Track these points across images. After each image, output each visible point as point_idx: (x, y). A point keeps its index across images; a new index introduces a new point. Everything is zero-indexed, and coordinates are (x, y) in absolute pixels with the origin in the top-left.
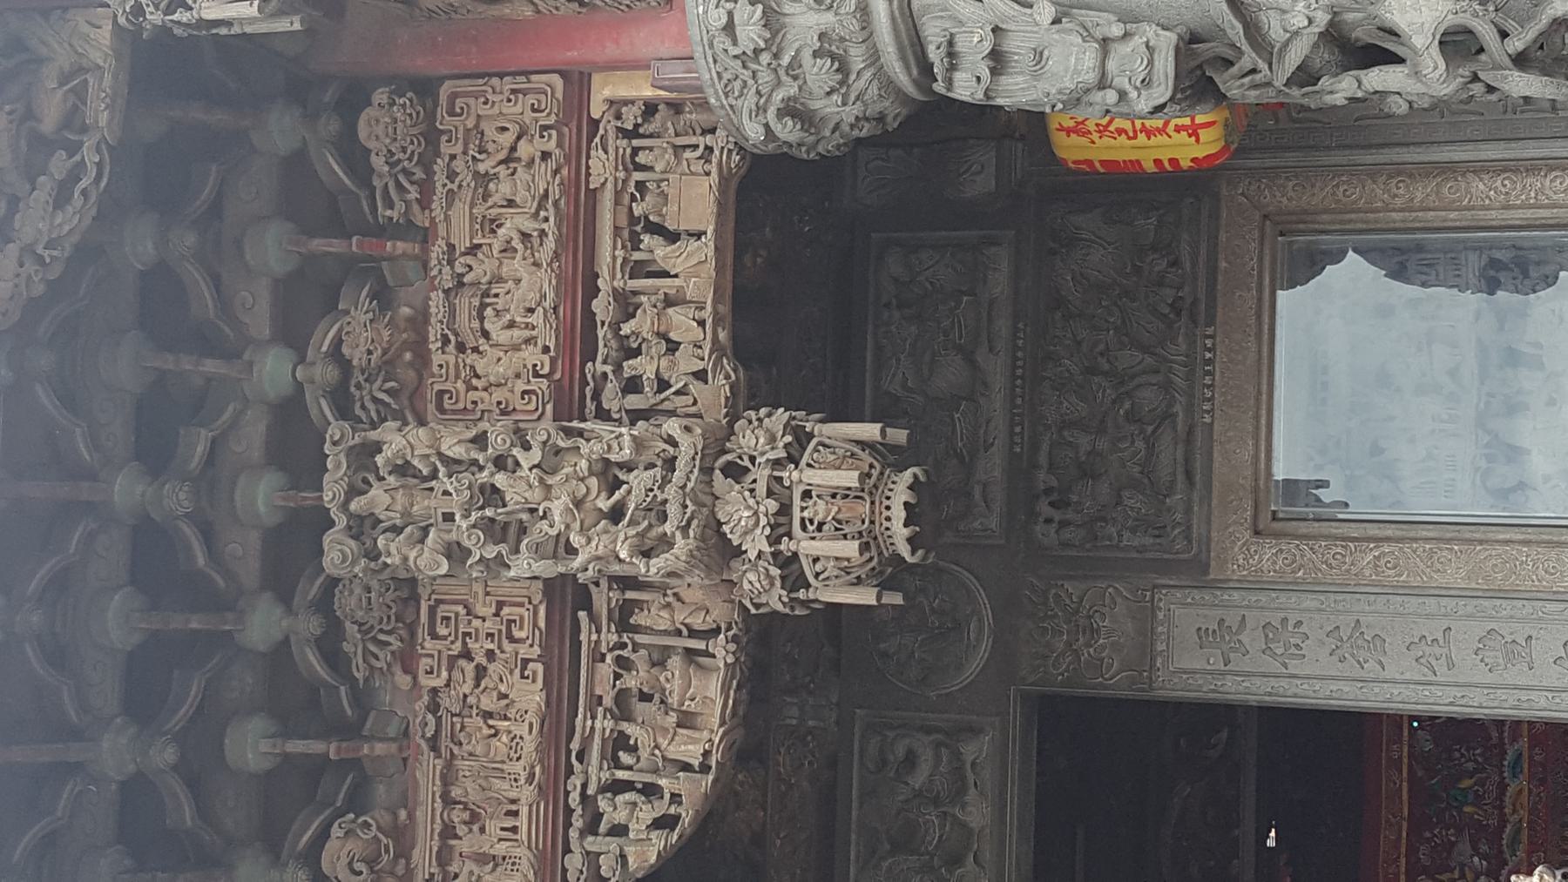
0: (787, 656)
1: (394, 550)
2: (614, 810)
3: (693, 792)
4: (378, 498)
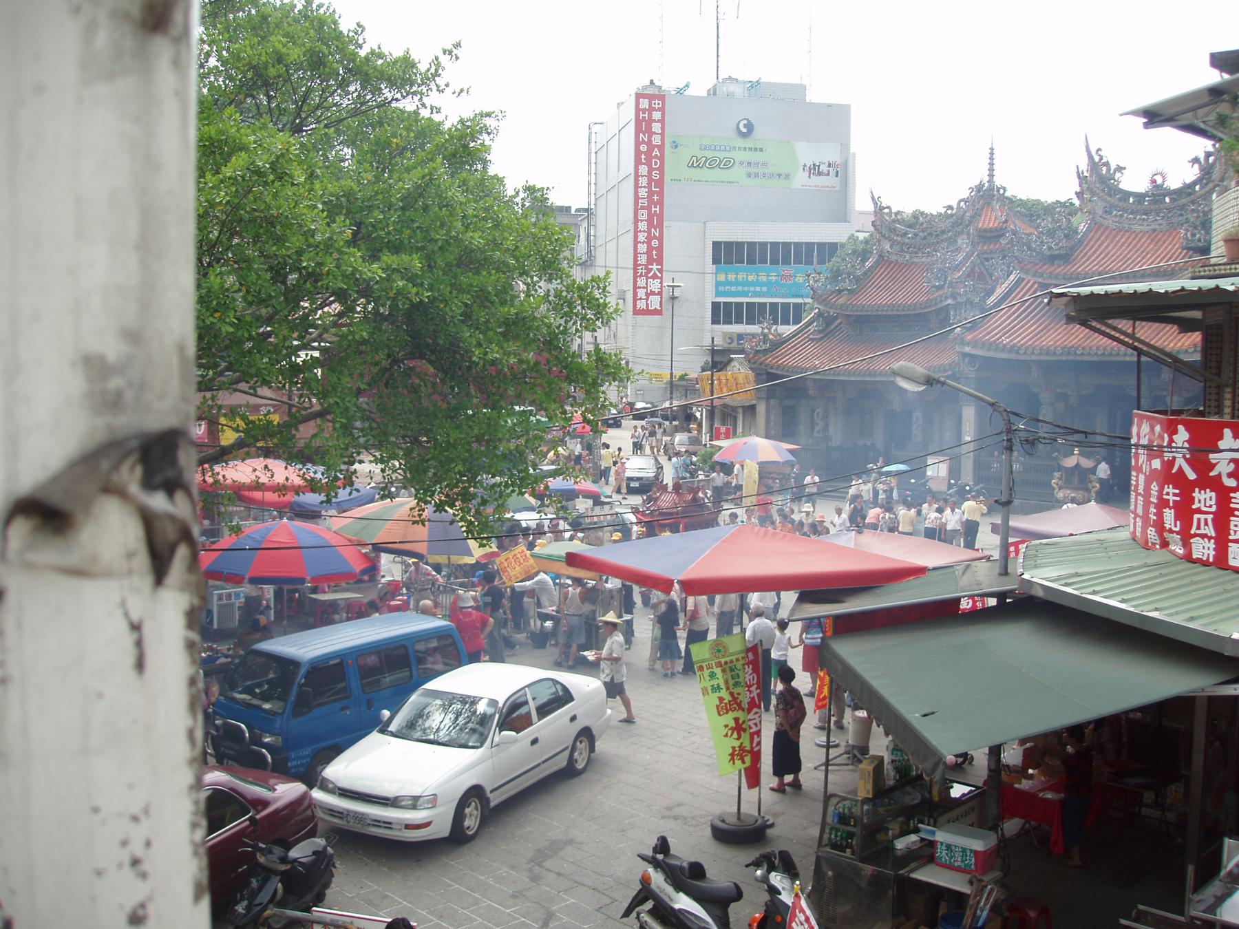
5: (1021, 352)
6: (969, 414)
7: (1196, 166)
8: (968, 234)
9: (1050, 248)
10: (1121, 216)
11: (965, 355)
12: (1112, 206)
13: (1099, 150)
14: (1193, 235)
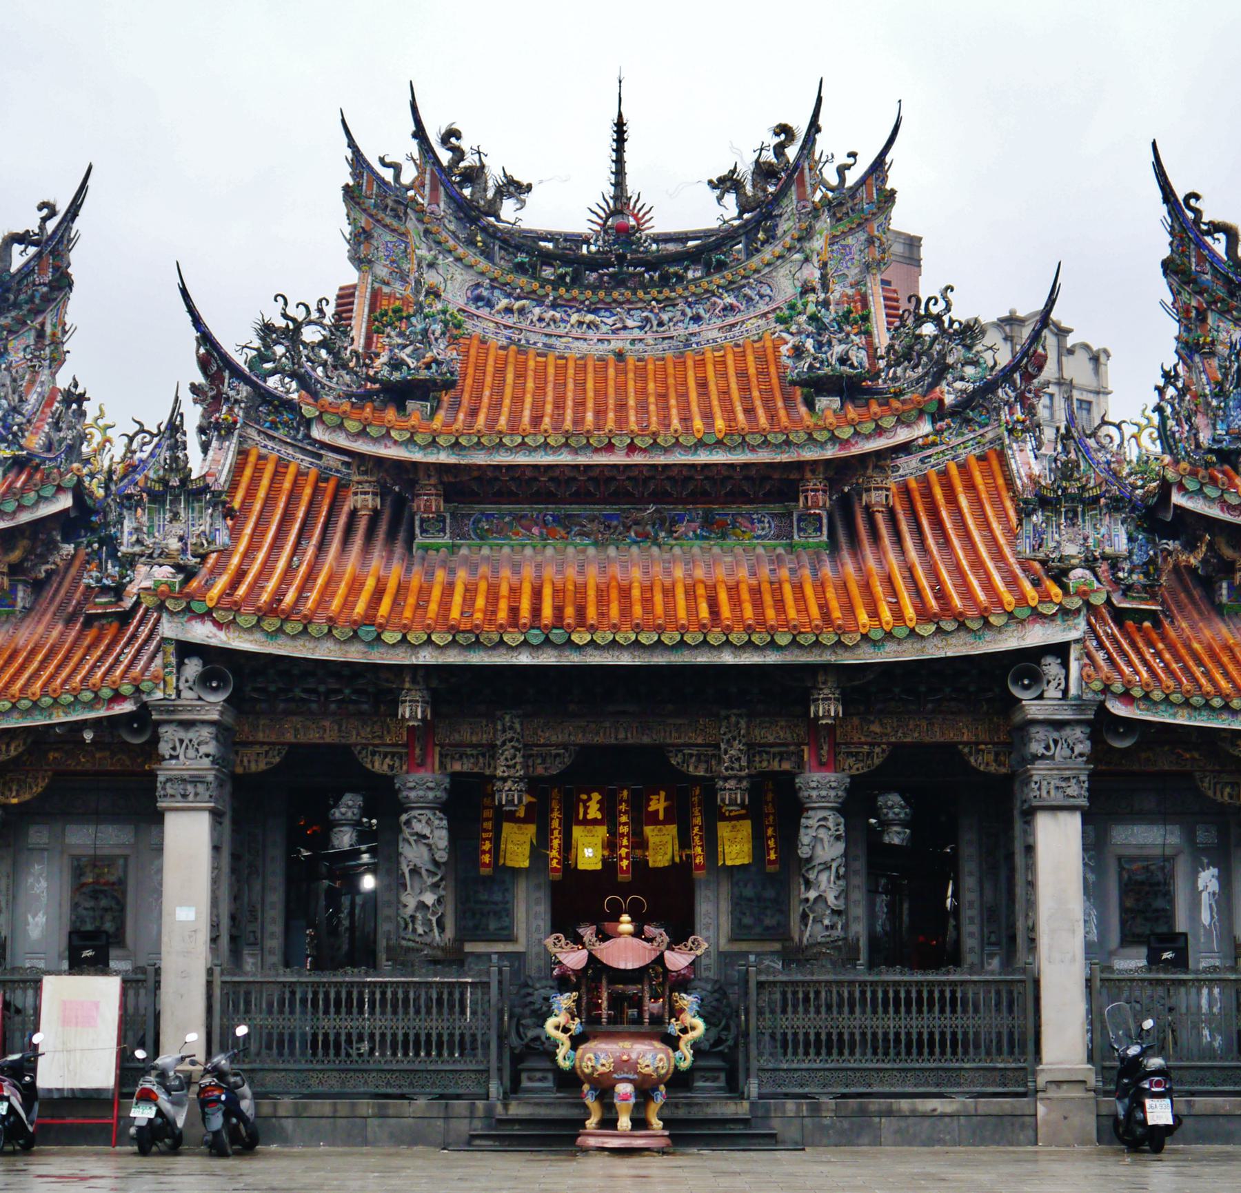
1: (724, 723)
2: (680, 755)
4: (733, 719)
5: (391, 637)
6: (189, 842)
7: (730, 199)
8: (40, 335)
9: (396, 364)
10: (522, 311)
11: (186, 650)
13: (451, 135)
14: (819, 346)
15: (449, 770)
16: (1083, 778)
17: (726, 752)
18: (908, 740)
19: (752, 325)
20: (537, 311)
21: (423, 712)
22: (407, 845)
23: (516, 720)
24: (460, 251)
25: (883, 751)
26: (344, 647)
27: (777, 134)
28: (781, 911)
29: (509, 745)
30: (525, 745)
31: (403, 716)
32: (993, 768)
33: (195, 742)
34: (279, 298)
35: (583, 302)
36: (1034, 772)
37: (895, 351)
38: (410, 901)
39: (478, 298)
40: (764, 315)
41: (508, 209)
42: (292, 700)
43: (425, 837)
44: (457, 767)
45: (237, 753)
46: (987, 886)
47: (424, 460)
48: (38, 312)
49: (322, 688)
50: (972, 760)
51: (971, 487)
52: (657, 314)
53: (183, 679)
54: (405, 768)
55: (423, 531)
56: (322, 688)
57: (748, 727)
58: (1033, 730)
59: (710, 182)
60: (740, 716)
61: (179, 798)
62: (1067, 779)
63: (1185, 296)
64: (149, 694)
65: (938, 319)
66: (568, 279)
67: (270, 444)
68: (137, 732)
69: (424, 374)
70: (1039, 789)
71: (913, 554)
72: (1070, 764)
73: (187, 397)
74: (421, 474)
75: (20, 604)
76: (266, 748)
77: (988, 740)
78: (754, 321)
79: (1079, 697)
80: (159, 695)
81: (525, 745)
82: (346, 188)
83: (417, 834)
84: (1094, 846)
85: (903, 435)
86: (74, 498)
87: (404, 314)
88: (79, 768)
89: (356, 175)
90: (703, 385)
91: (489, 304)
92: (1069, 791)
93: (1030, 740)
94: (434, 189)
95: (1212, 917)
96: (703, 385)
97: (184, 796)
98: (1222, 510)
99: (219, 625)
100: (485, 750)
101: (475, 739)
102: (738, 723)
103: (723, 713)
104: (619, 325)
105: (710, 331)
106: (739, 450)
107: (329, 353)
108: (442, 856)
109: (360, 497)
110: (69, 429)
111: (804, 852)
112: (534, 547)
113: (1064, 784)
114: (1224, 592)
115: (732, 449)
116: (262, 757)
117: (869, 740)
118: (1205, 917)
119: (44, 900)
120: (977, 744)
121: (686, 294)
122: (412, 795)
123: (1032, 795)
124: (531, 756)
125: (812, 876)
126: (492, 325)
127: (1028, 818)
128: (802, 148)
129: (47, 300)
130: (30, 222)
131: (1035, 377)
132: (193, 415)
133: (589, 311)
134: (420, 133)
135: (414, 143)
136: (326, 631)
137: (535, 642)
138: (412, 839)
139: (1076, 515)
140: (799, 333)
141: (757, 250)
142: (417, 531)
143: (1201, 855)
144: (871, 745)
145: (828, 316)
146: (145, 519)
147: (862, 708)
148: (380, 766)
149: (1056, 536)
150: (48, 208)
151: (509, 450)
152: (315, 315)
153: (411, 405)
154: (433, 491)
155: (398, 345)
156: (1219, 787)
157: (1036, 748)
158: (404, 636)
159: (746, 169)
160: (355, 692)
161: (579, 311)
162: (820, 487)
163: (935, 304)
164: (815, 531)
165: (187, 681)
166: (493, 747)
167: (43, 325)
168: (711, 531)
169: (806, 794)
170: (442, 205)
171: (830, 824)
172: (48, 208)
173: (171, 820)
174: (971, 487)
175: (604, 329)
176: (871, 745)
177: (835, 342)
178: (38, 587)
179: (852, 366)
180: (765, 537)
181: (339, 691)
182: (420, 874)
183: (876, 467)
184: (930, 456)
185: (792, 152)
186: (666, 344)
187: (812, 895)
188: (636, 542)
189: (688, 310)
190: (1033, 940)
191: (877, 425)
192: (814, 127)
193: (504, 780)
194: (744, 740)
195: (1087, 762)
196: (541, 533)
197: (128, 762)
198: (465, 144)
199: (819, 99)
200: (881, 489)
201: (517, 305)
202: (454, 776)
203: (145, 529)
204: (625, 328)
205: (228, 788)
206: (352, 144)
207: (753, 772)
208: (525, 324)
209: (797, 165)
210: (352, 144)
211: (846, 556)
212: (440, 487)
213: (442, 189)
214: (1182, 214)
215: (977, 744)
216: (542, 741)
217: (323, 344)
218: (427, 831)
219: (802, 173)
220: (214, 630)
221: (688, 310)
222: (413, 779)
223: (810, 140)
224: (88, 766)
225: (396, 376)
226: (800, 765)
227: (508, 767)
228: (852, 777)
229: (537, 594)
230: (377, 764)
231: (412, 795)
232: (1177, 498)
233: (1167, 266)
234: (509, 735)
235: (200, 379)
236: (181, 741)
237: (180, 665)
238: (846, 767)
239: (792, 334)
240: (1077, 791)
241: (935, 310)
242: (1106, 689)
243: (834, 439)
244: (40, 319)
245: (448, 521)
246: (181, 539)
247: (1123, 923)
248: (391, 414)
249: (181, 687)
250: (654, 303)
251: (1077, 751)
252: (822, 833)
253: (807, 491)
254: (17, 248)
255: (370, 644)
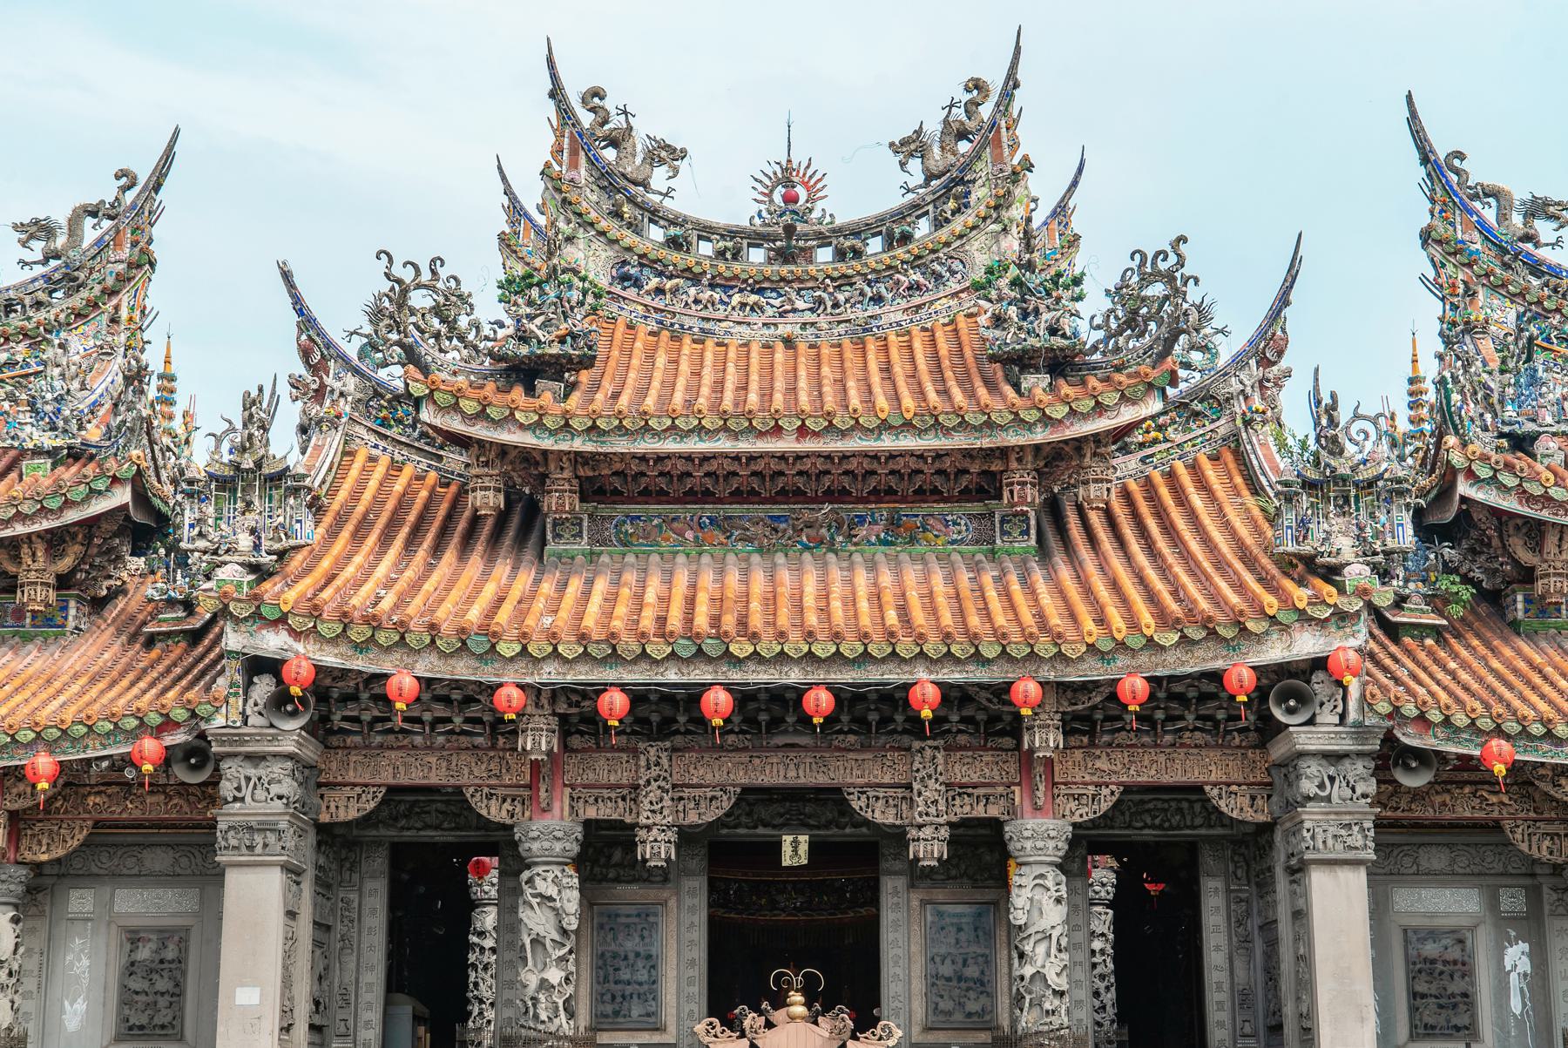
0: (898, 837)
1: (918, 758)
2: (864, 797)
3: (869, 816)
4: (928, 752)
7: (915, 165)
9: (523, 338)
10: (675, 291)
11: (258, 666)
12: (645, 261)
14: (1024, 315)
15: (582, 817)
16: (1368, 824)
17: (920, 794)
18: (1143, 779)
19: (942, 305)
20: (692, 291)
21: (548, 743)
22: (529, 912)
23: (664, 755)
24: (603, 225)
25: (1112, 793)
26: (452, 662)
27: (968, 90)
28: (988, 994)
29: (654, 785)
30: (674, 786)
31: (524, 749)
32: (1249, 815)
33: (265, 780)
34: (383, 256)
35: (745, 281)
36: (1304, 817)
37: (1117, 318)
38: (532, 980)
39: (624, 278)
40: (955, 295)
41: (659, 178)
42: (391, 731)
43: (551, 899)
44: (592, 813)
45: (322, 797)
46: (1239, 964)
47: (556, 448)
48: (113, 293)
49: (427, 717)
50: (1222, 803)
51: (1203, 485)
52: (831, 294)
53: (251, 702)
54: (527, 814)
55: (557, 536)
56: (427, 717)
57: (946, 763)
58: (1302, 764)
59: (892, 145)
60: (936, 748)
61: (244, 850)
62: (1348, 826)
63: (1450, 269)
64: (208, 720)
65: (1169, 277)
66: (728, 255)
67: (382, 444)
68: (196, 768)
69: (555, 349)
70: (1313, 838)
71: (1142, 559)
72: (1350, 806)
73: (284, 390)
74: (552, 466)
75: (71, 623)
76: (358, 790)
77: (1241, 780)
78: (944, 301)
79: (1358, 724)
80: (220, 720)
81: (674, 786)
82: (503, 238)
83: (540, 895)
84: (1379, 909)
85: (1127, 415)
86: (134, 491)
87: (535, 280)
88: (124, 816)
89: (512, 223)
90: (887, 370)
91: (637, 284)
92: (1349, 841)
93: (1298, 777)
94: (574, 153)
95: (1524, 1005)
96: (887, 370)
97: (251, 848)
98: (1520, 503)
99: (296, 634)
100: (625, 792)
101: (613, 779)
102: (934, 757)
103: (917, 745)
104: (788, 307)
105: (892, 313)
106: (931, 434)
107: (442, 321)
108: (572, 923)
109: (479, 494)
110: (128, 410)
111: (1018, 918)
112: (688, 555)
113: (1343, 832)
114: (1520, 606)
115: (921, 432)
116: (353, 802)
117: (1095, 779)
118: (1516, 1005)
119: (85, 982)
120: (1229, 785)
121: (866, 270)
122: (535, 846)
123: (1304, 845)
124: (681, 798)
125: (1028, 948)
126: (640, 308)
127: (1298, 876)
128: (998, 105)
129: (123, 279)
130: (107, 191)
131: (1274, 363)
132: (289, 415)
133: (752, 292)
134: (556, 93)
135: (551, 103)
136: (428, 641)
137: (685, 654)
138: (534, 901)
139: (1347, 500)
140: (1000, 299)
141: (947, 221)
142: (549, 536)
143: (1506, 926)
144: (1098, 785)
145: (1033, 280)
146: (211, 510)
147: (1085, 740)
148: (496, 812)
149: (1326, 526)
150: (127, 178)
151: (656, 434)
152: (426, 276)
153: (540, 384)
154: (567, 487)
155: (528, 316)
156: (1535, 839)
157: (1308, 787)
158: (524, 648)
159: (933, 127)
160: (468, 720)
161: (741, 291)
162: (1028, 479)
163: (1165, 259)
164: (1022, 533)
165: (256, 704)
166: (636, 787)
167: (117, 308)
168: (898, 536)
169: (1019, 846)
170: (583, 172)
171: (1050, 883)
172: (127, 178)
173: (233, 879)
174: (1203, 485)
175: (770, 311)
176: (1098, 785)
177: (1042, 308)
178: (98, 605)
179: (1064, 336)
180: (961, 542)
181: (449, 720)
182: (544, 945)
183: (1095, 454)
184: (1152, 456)
185: (986, 111)
186: (842, 328)
187: (1028, 971)
188: (807, 548)
189: (867, 289)
190: (1308, 1030)
191: (1097, 403)
192: (1012, 82)
193: (649, 828)
194: (941, 779)
195: (1371, 805)
196: (696, 538)
197: (186, 808)
198: (609, 104)
199: (1018, 49)
200: (1101, 481)
201: (669, 284)
202: (588, 824)
203: (210, 521)
204: (794, 310)
205: (311, 838)
206: (508, 191)
207: (954, 819)
208: (678, 308)
209: (994, 125)
210: (508, 191)
211: (1059, 559)
212: (575, 482)
213: (582, 154)
214: (1441, 175)
215: (1229, 785)
216: (695, 781)
217: (437, 311)
218: (552, 891)
219: (998, 131)
220: (290, 641)
221: (867, 289)
222: (537, 826)
223: (1008, 94)
224: (137, 814)
225: (524, 350)
226: (1012, 812)
227: (653, 812)
228: (1074, 825)
229: (691, 602)
230: (493, 810)
231: (535, 846)
232: (1463, 488)
233: (1426, 237)
234: (655, 771)
235: (300, 369)
236: (248, 779)
237: (249, 684)
238: (1067, 813)
239: (990, 301)
240: (1363, 843)
241: (1163, 266)
242: (1396, 713)
243: (1046, 420)
244: (114, 301)
245: (585, 524)
246: (253, 531)
247: (1413, 1010)
248: (518, 393)
249: (249, 712)
250: (828, 281)
251: (1359, 791)
252: (1039, 894)
253: (1012, 484)
254: (89, 222)
255: (480, 657)
